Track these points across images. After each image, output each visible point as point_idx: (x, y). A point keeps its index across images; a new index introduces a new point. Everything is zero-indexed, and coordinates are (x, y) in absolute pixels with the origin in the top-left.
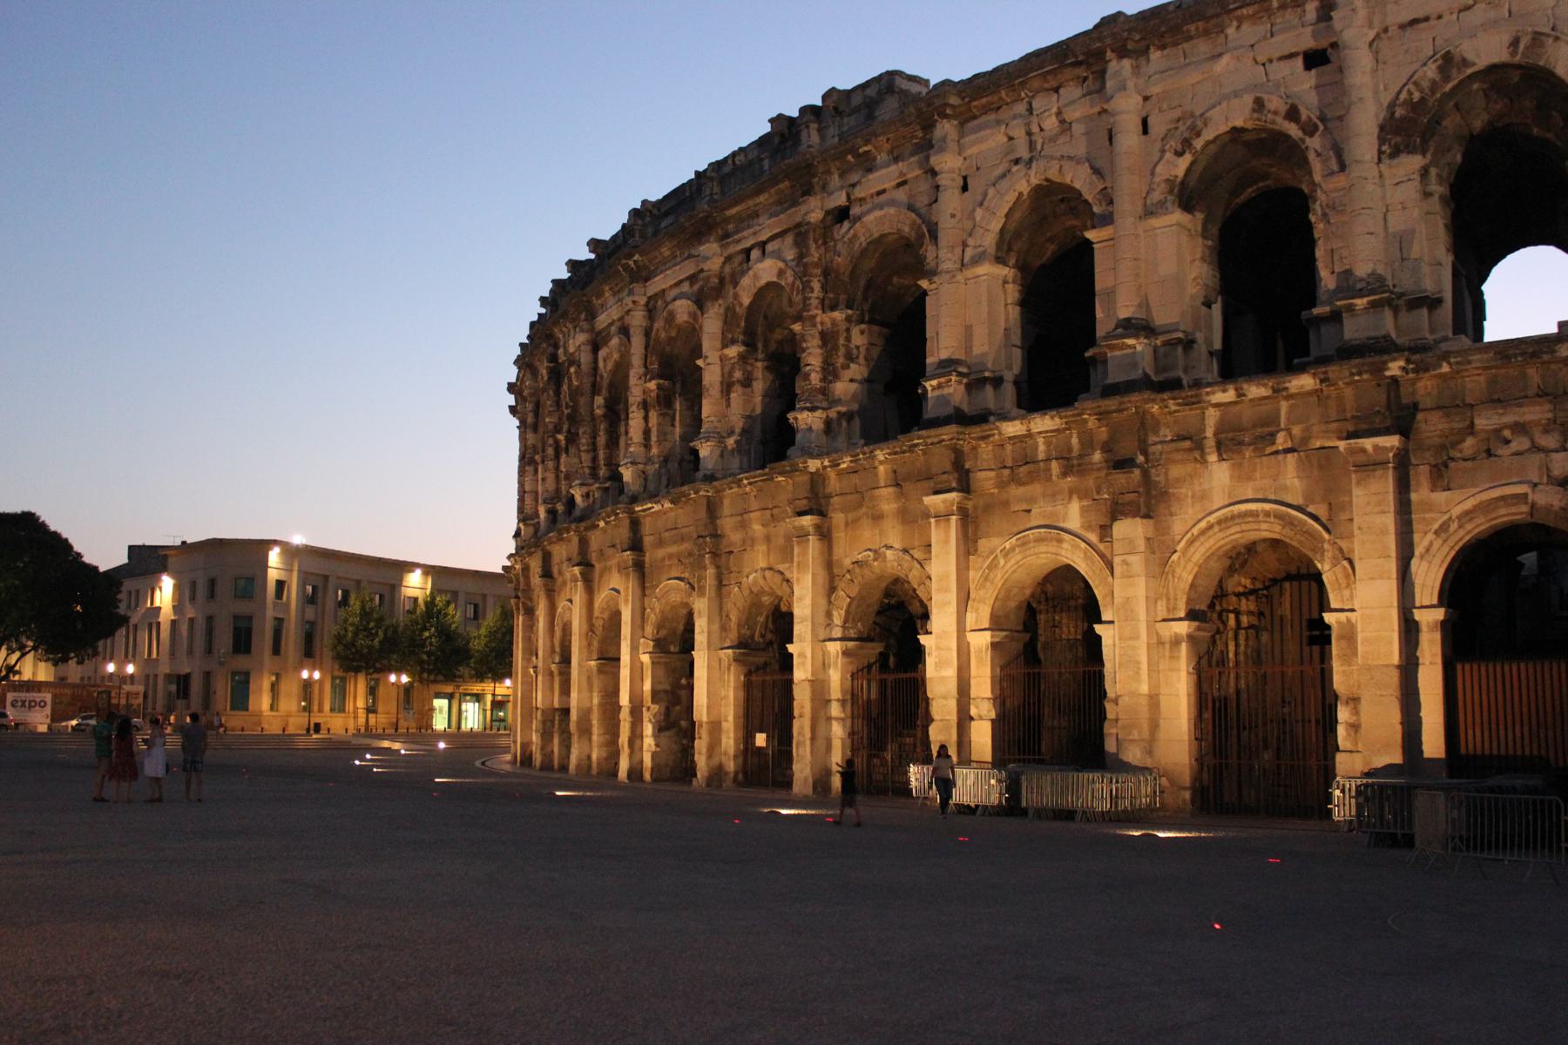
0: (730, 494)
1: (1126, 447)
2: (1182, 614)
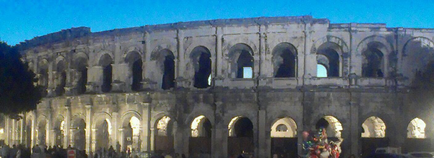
0: (54, 101)
1: (115, 101)
2: (122, 127)
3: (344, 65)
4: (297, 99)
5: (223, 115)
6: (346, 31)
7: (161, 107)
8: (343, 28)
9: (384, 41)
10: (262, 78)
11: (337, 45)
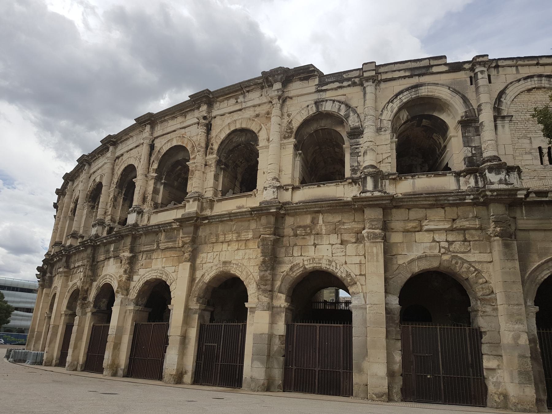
4: (250, 236)
8: (349, 79)
9: (444, 93)
10: (191, 198)
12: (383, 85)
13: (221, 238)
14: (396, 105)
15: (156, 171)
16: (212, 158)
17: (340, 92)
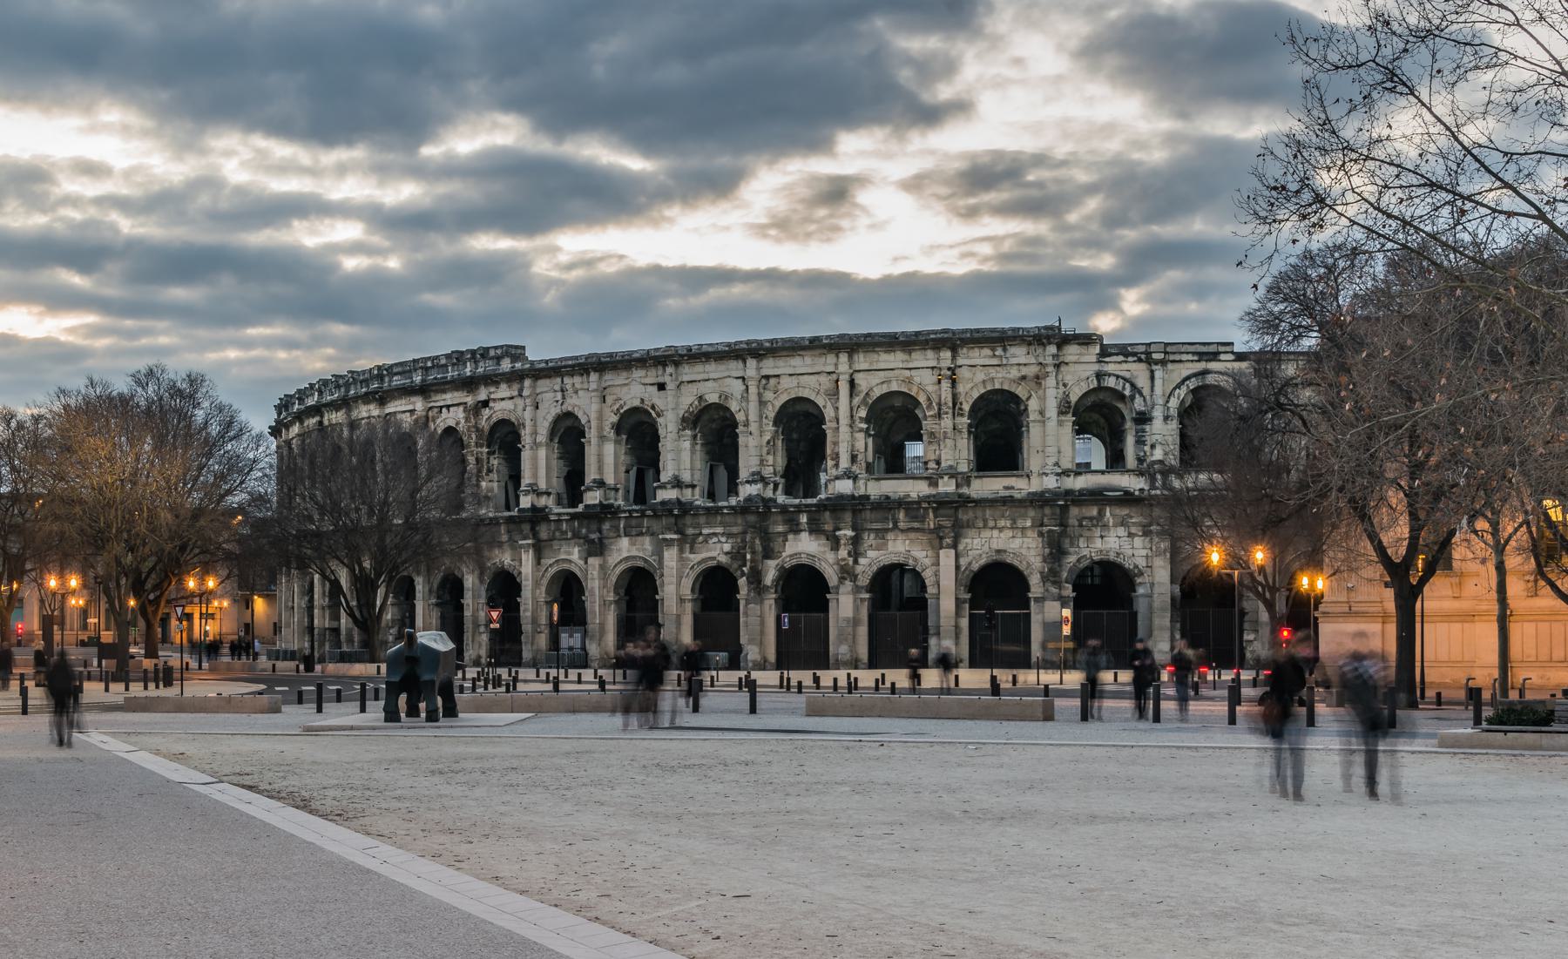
3: (1140, 442)
4: (1029, 524)
5: (856, 562)
6: (1140, 360)
7: (706, 541)
8: (1134, 354)
11: (1122, 397)
12: (1170, 366)
13: (991, 523)
14: (1183, 392)
15: (867, 420)
16: (965, 420)
17: (1125, 366)
